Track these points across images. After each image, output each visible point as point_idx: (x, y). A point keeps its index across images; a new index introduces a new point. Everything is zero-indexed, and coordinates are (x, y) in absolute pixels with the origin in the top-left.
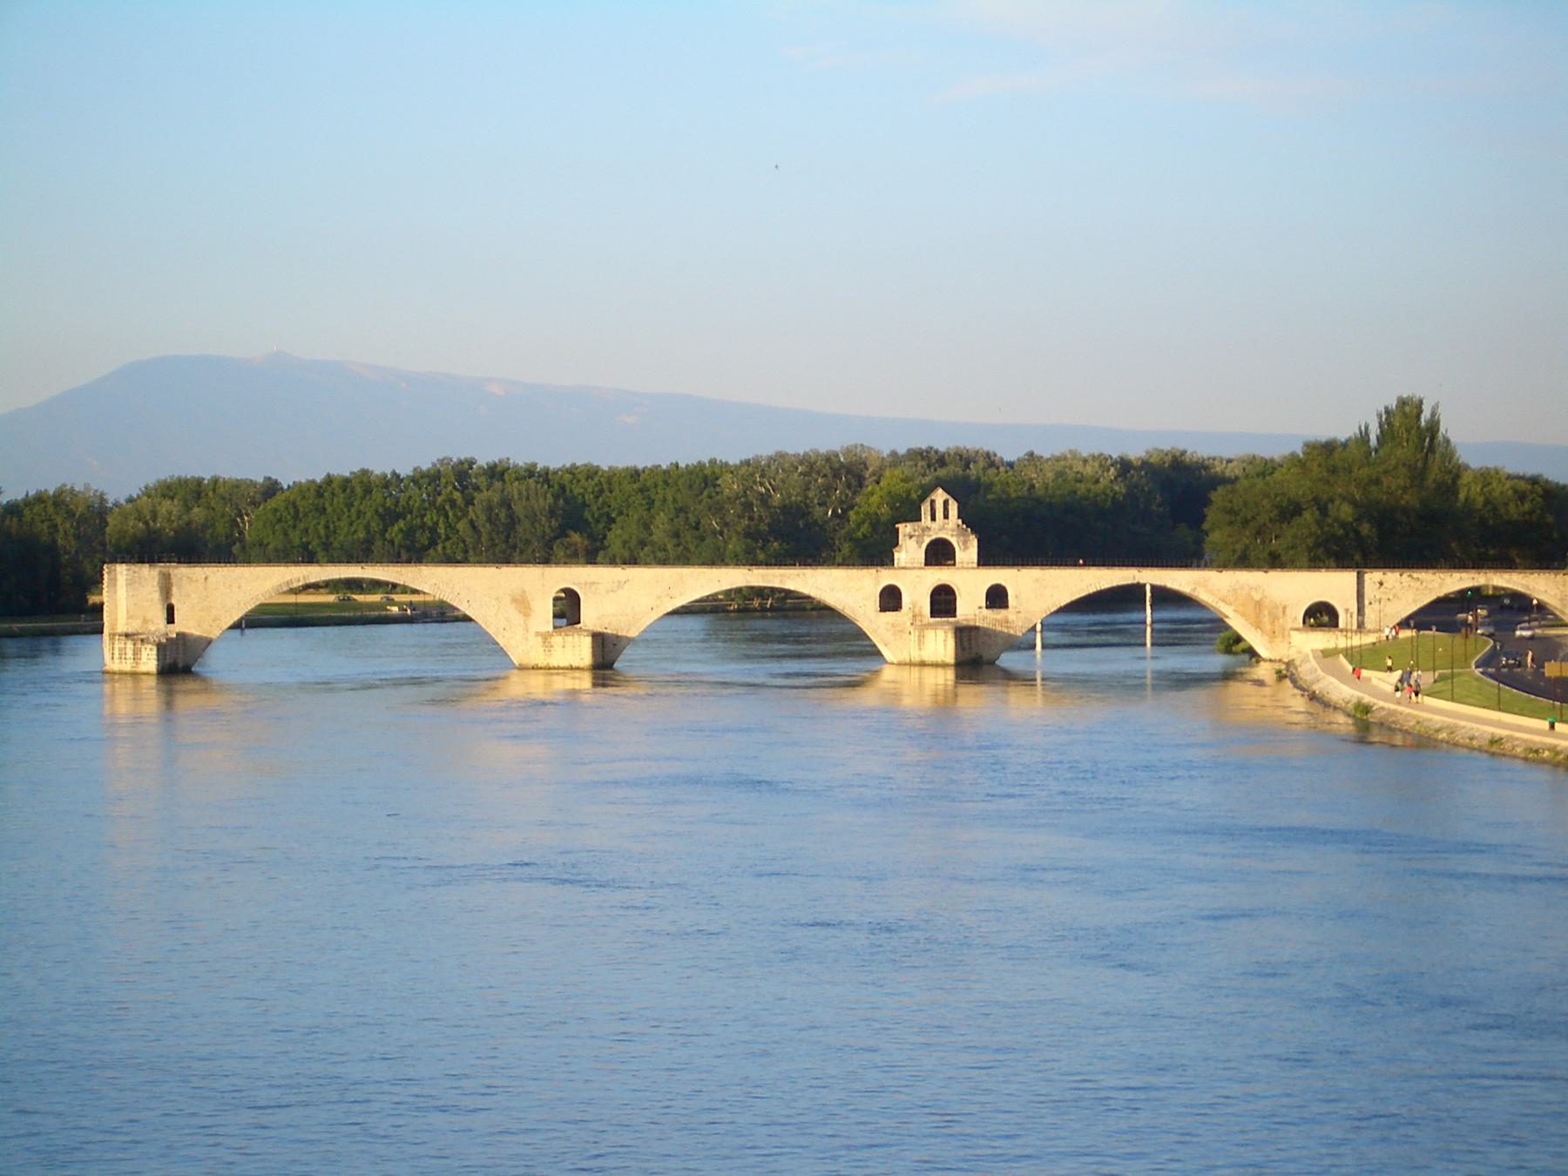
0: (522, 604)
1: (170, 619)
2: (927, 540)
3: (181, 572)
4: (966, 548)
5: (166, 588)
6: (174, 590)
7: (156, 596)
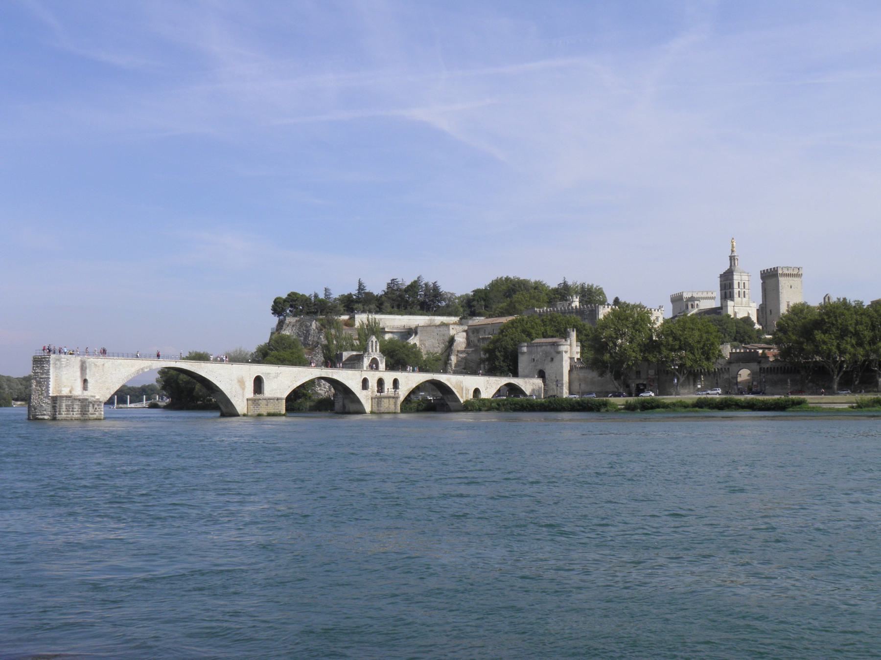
0: (241, 382)
1: (85, 388)
3: (91, 360)
5: (83, 368)
6: (88, 371)
7: (78, 373)
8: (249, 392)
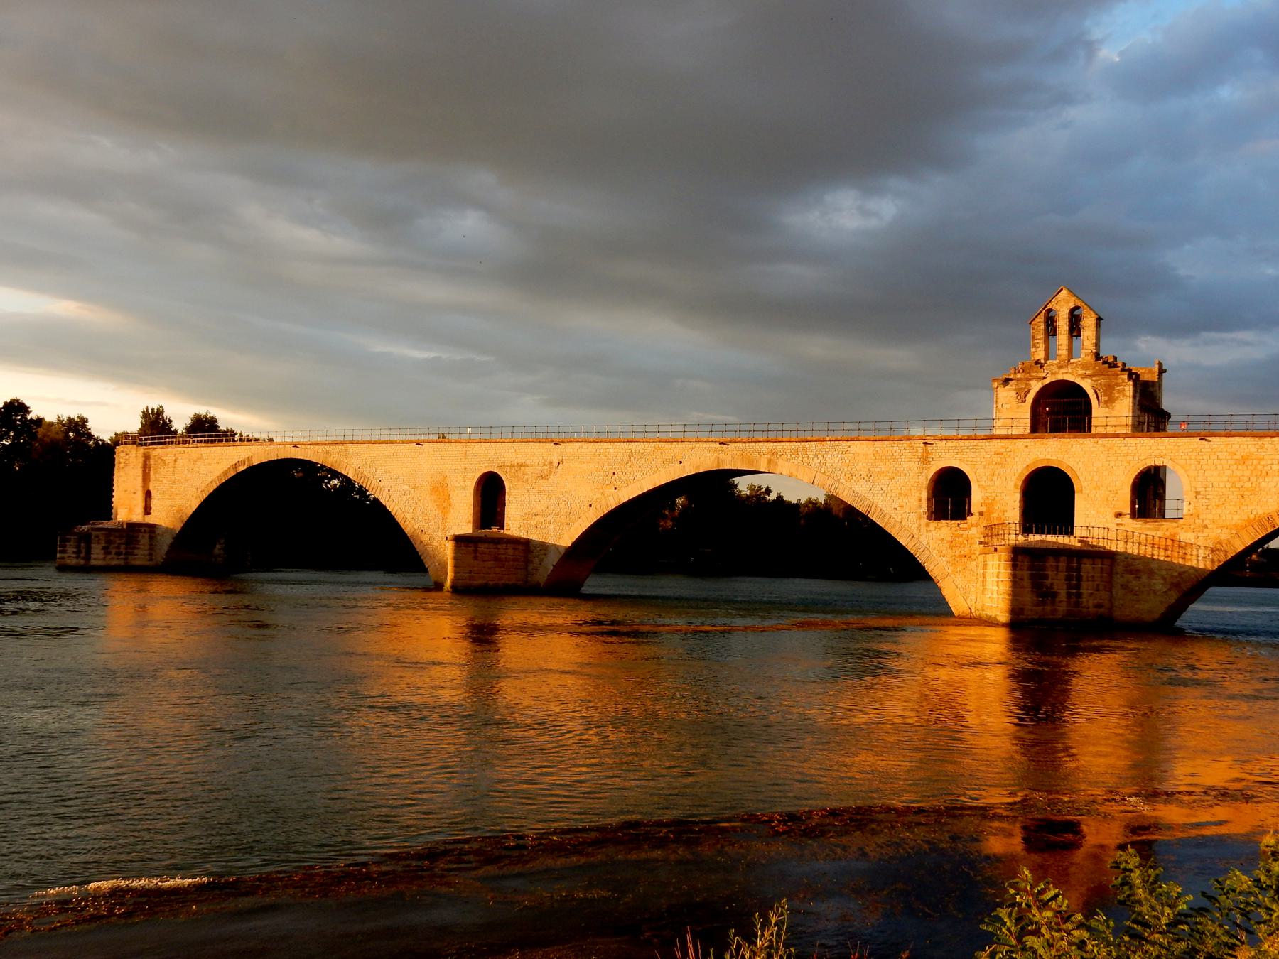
0: (441, 490)
1: (147, 510)
2: (1036, 387)
4: (1110, 402)
7: (140, 479)
8: (463, 522)
